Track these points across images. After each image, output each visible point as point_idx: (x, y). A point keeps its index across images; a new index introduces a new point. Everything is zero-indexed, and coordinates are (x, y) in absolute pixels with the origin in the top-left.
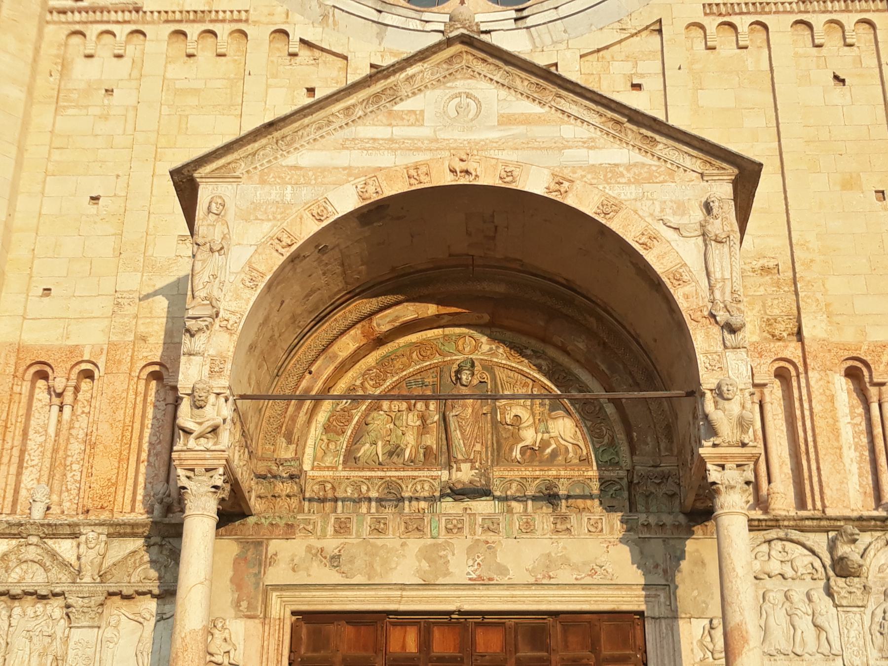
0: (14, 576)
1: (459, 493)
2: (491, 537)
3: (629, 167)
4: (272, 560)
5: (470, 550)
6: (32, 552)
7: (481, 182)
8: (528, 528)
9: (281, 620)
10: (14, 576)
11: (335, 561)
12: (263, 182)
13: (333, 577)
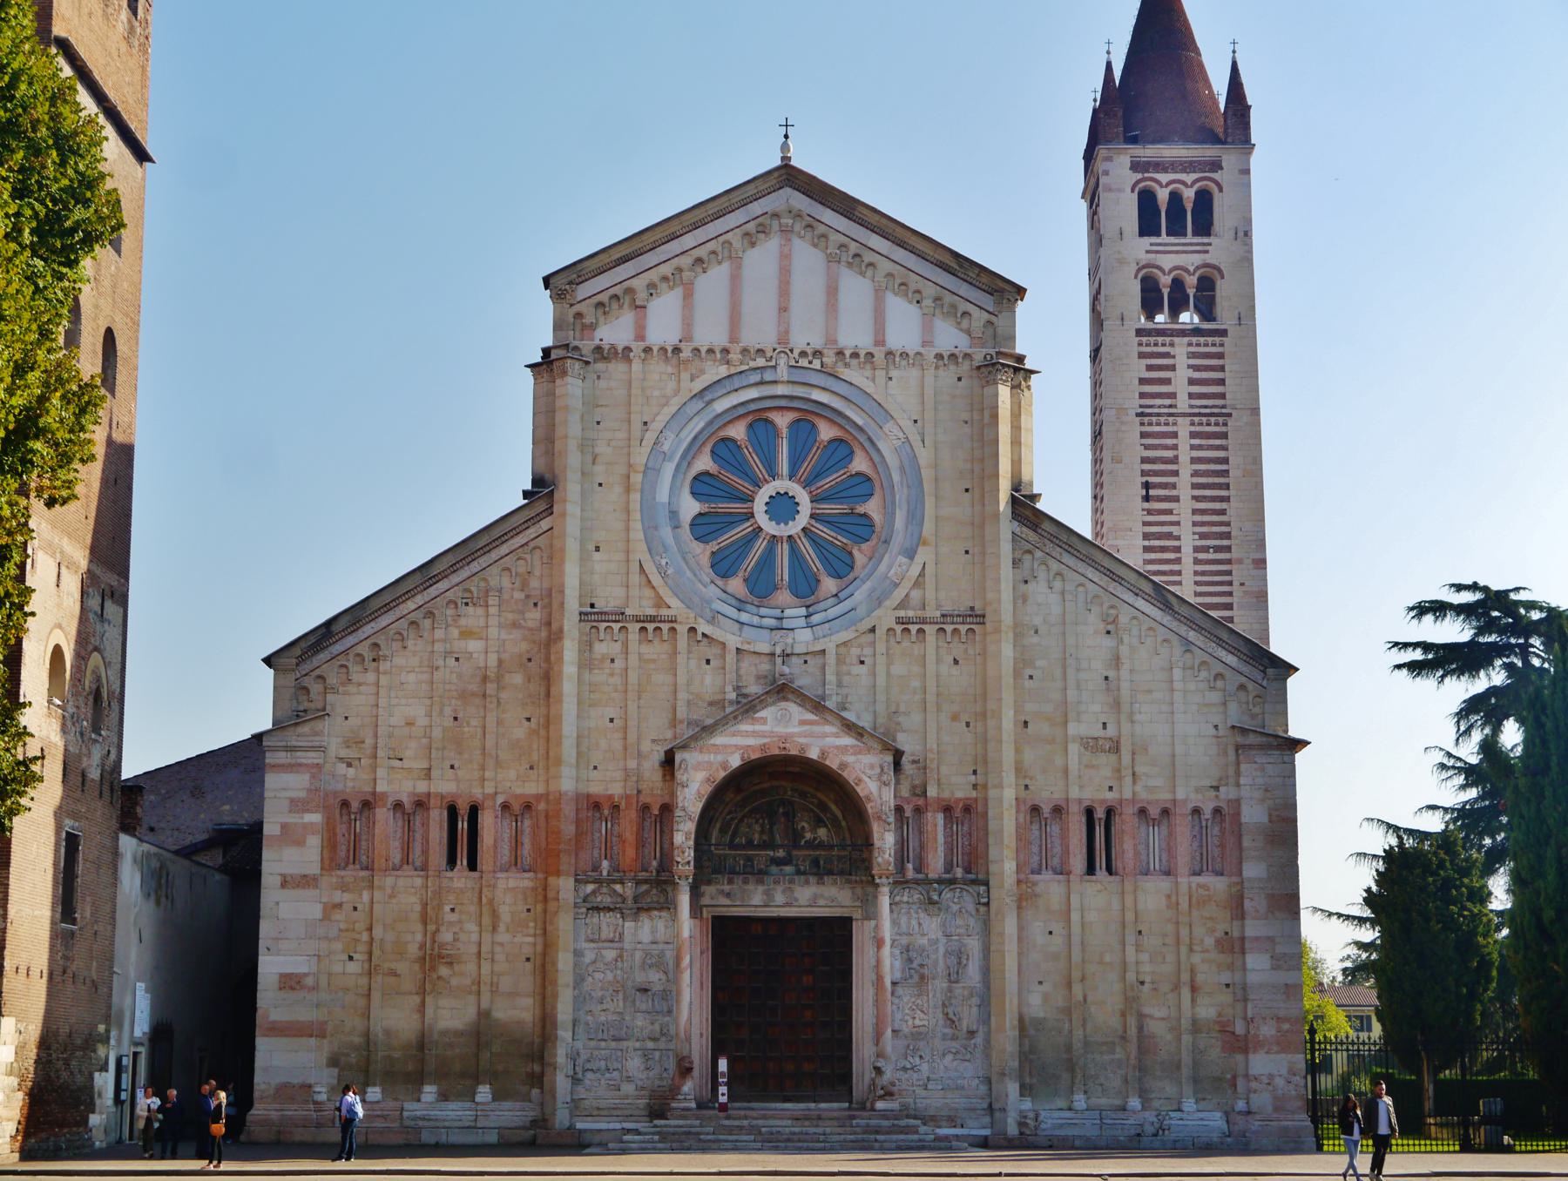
0: (599, 899)
1: (779, 862)
2: (792, 886)
3: (852, 747)
4: (702, 895)
5: (784, 892)
6: (604, 890)
7: (791, 753)
8: (807, 882)
9: (707, 919)
10: (599, 899)
11: (728, 895)
12: (701, 752)
13: (728, 902)
